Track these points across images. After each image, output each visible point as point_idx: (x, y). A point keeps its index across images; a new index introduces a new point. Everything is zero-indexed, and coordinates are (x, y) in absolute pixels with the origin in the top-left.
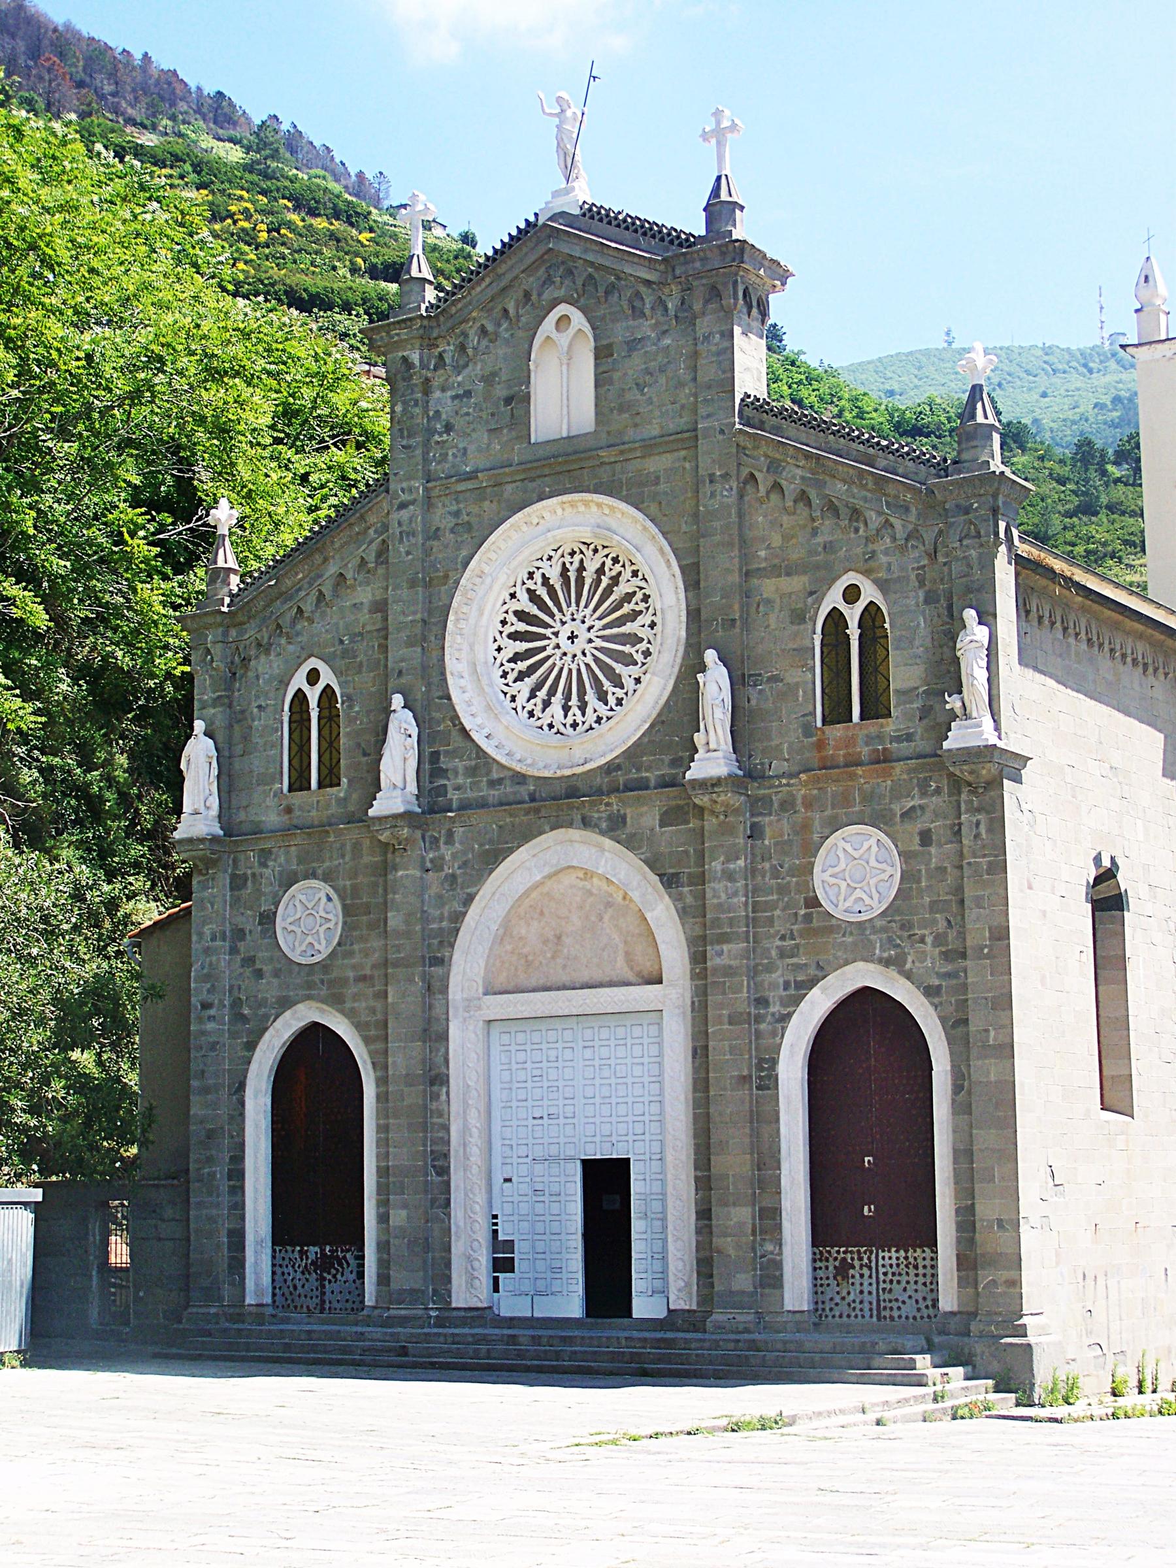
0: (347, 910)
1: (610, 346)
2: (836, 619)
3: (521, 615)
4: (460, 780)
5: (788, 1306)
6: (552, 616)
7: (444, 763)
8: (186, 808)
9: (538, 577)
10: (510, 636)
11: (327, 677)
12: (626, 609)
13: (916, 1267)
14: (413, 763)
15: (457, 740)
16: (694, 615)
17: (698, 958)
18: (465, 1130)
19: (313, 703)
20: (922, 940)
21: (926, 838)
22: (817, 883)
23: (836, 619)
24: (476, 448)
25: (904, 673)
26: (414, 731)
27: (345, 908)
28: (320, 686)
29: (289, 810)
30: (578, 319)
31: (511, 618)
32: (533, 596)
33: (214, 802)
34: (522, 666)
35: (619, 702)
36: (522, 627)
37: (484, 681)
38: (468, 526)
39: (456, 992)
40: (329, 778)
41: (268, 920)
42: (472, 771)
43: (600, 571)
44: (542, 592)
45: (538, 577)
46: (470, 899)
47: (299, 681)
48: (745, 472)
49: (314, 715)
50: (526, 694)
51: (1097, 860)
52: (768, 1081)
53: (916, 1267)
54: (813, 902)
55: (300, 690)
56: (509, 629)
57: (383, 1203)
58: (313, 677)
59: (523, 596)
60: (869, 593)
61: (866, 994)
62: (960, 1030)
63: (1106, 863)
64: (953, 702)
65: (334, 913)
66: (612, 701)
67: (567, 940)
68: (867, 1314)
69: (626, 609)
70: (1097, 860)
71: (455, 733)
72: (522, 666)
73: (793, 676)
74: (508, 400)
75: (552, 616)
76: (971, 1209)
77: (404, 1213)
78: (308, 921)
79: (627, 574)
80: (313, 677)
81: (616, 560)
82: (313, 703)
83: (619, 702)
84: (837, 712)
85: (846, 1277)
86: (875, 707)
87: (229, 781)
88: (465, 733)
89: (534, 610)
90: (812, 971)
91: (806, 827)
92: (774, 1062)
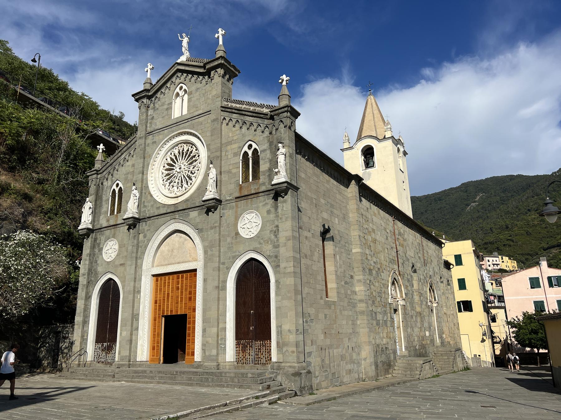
0: (120, 247)
1: (191, 92)
2: (246, 153)
3: (168, 164)
4: (149, 208)
5: (227, 360)
6: (175, 163)
7: (146, 204)
8: (82, 221)
9: (173, 154)
10: (166, 170)
11: (121, 185)
12: (194, 159)
13: (265, 347)
14: (137, 204)
15: (149, 197)
16: (208, 157)
17: (205, 252)
18: (144, 307)
19: (117, 192)
20: (268, 243)
21: (269, 212)
22: (239, 228)
23: (246, 153)
24: (159, 123)
25: (264, 166)
26: (138, 195)
27: (119, 245)
28: (119, 187)
29: (108, 221)
30: (184, 87)
31: (166, 165)
32: (172, 159)
33: (90, 218)
34: (167, 177)
35: (191, 184)
36: (168, 167)
37: (158, 182)
38: (155, 142)
39: (144, 267)
40: (119, 211)
41: (101, 250)
42: (152, 206)
43: (188, 150)
44: (174, 158)
45: (173, 154)
46: (149, 240)
47: (114, 187)
48: (222, 117)
49: (117, 195)
50: (168, 184)
51: (324, 226)
52: (224, 288)
53: (265, 347)
54: (237, 234)
55: (114, 189)
56: (165, 168)
57: (121, 330)
58: (117, 185)
59: (169, 160)
60: (254, 146)
61: (252, 259)
62: (278, 269)
63: (327, 227)
64: (276, 170)
65: (117, 247)
66: (189, 184)
67: (175, 251)
68: (251, 362)
69: (194, 159)
70: (324, 226)
71: (149, 196)
72: (167, 177)
73: (234, 171)
74: (167, 109)
75: (175, 163)
76: (281, 326)
77: (125, 332)
78: (110, 250)
79: (194, 150)
80: (117, 185)
81: (192, 147)
82: (117, 192)
83: (191, 184)
84: (246, 179)
85: (245, 351)
86: (256, 175)
87: (95, 213)
88: (151, 196)
89: (172, 162)
90: (237, 254)
91: (236, 212)
92: (225, 282)
